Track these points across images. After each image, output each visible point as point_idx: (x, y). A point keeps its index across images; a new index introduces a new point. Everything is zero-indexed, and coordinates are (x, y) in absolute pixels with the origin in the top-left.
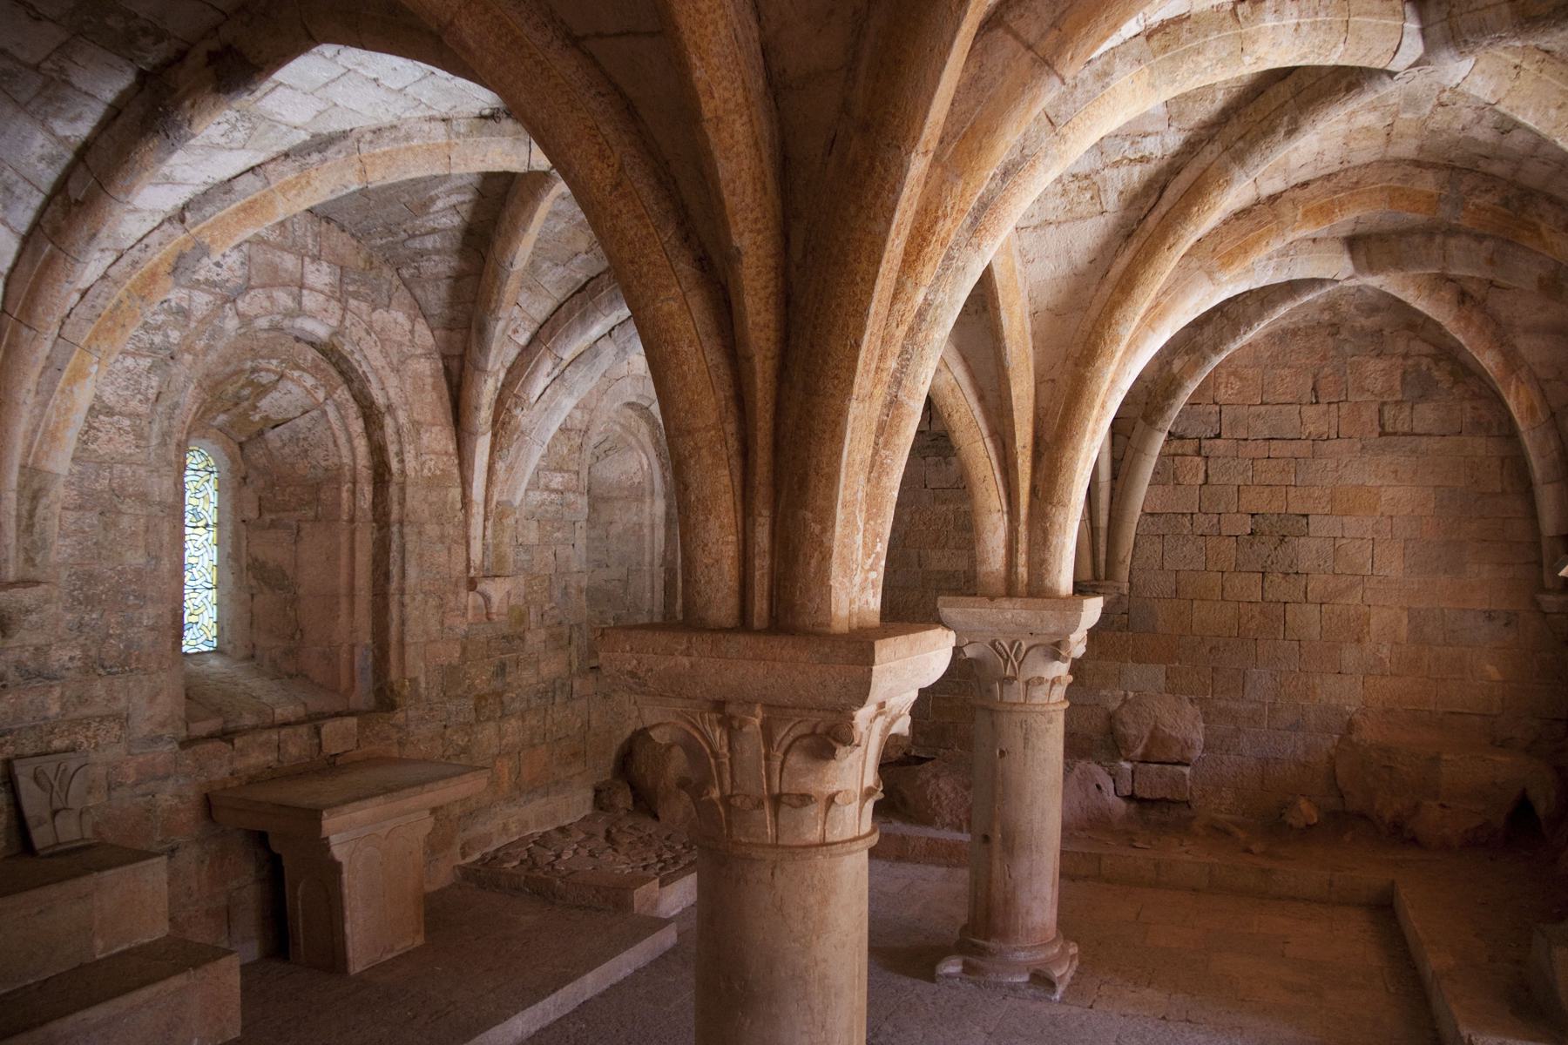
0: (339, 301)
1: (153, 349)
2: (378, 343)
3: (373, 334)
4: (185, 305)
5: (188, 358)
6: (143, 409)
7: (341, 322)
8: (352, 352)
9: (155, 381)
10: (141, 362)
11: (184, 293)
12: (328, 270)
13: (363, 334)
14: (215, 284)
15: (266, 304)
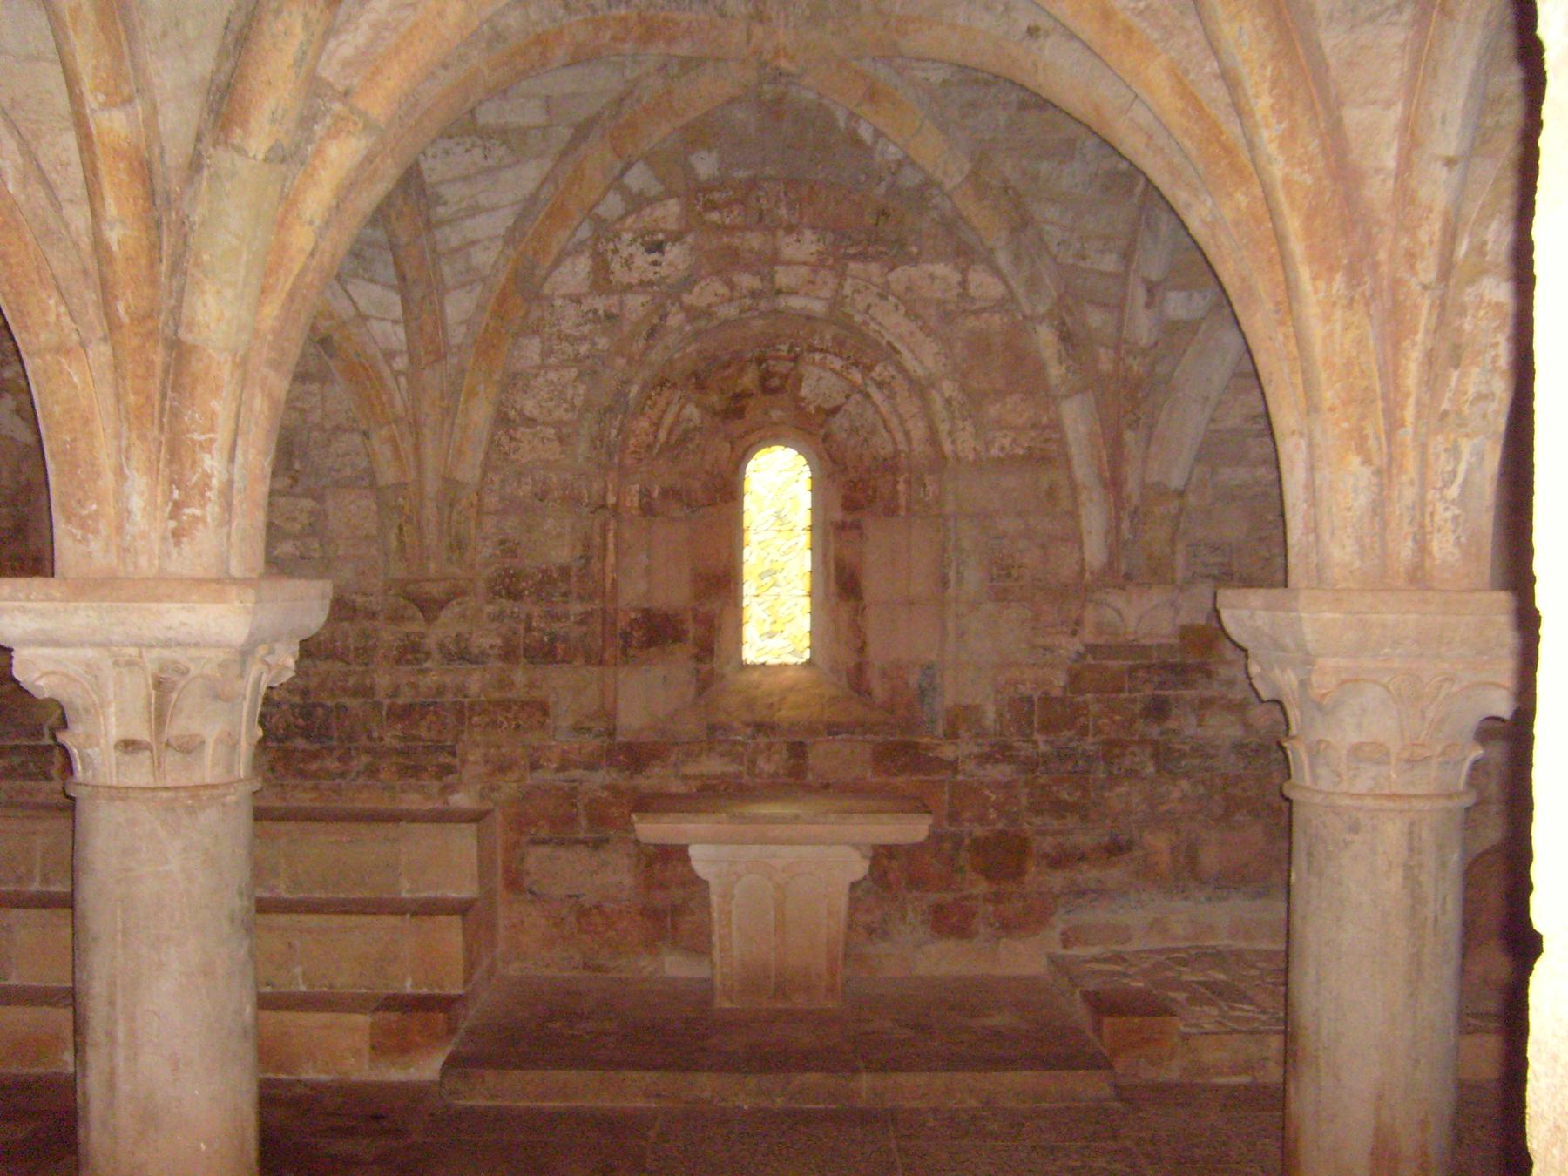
0: (831, 268)
1: (577, 359)
2: (901, 306)
3: (890, 298)
4: (615, 310)
5: (621, 362)
6: (569, 416)
7: (837, 291)
8: (865, 323)
9: (581, 389)
10: (565, 373)
11: (614, 300)
12: (814, 238)
13: (872, 299)
14: (651, 283)
15: (724, 290)
